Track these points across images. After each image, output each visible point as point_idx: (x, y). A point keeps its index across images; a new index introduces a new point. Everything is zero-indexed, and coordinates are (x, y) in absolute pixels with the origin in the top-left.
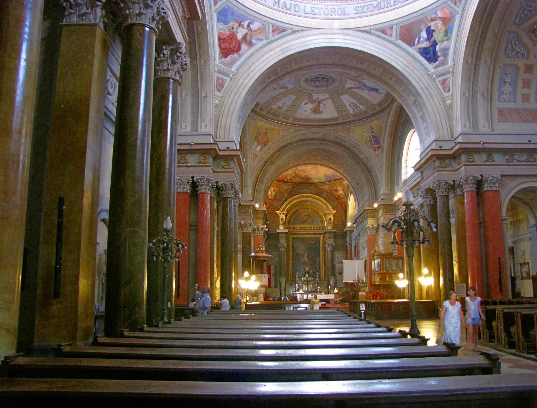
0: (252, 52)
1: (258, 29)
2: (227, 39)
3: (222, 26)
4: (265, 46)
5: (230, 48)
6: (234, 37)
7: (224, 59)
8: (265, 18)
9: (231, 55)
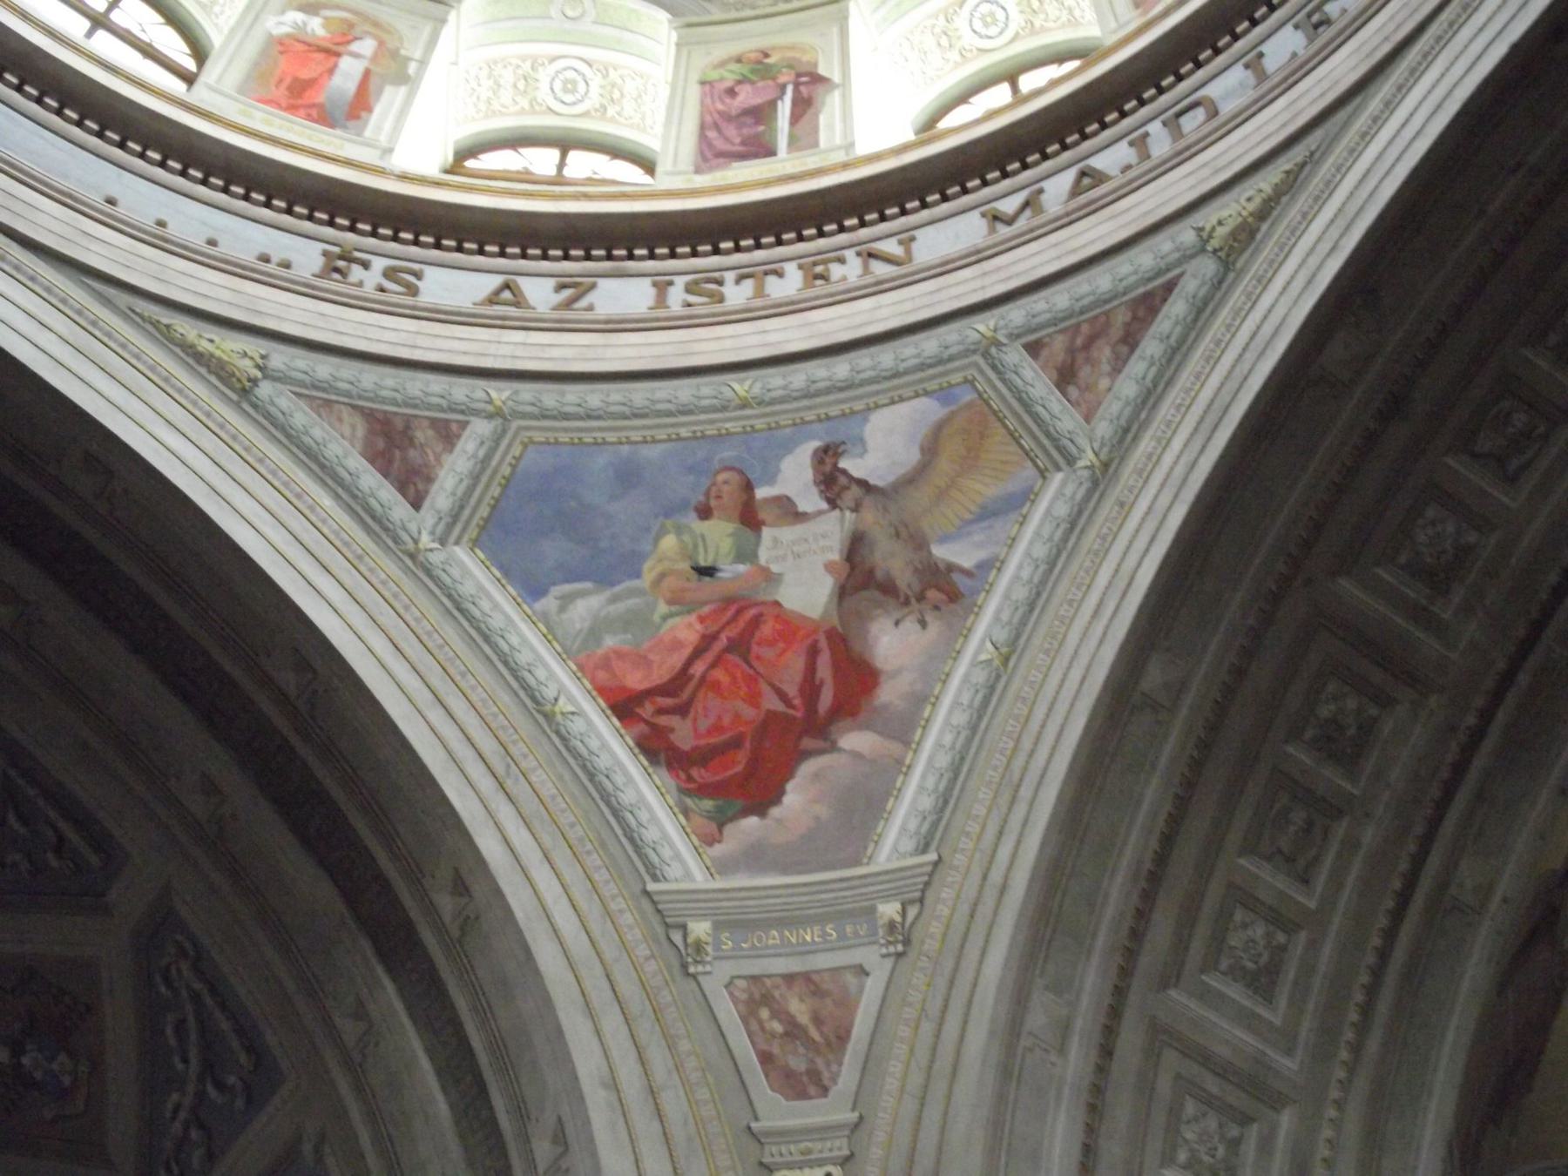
0: (1001, 635)
1: (931, 448)
2: (698, 669)
3: (587, 606)
4: (1075, 524)
5: (771, 716)
6: (756, 622)
7: (752, 821)
8: (928, 344)
9: (807, 768)
